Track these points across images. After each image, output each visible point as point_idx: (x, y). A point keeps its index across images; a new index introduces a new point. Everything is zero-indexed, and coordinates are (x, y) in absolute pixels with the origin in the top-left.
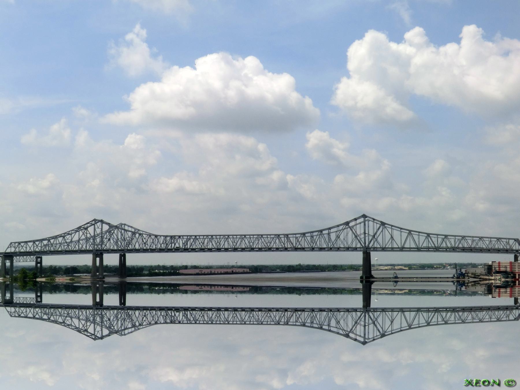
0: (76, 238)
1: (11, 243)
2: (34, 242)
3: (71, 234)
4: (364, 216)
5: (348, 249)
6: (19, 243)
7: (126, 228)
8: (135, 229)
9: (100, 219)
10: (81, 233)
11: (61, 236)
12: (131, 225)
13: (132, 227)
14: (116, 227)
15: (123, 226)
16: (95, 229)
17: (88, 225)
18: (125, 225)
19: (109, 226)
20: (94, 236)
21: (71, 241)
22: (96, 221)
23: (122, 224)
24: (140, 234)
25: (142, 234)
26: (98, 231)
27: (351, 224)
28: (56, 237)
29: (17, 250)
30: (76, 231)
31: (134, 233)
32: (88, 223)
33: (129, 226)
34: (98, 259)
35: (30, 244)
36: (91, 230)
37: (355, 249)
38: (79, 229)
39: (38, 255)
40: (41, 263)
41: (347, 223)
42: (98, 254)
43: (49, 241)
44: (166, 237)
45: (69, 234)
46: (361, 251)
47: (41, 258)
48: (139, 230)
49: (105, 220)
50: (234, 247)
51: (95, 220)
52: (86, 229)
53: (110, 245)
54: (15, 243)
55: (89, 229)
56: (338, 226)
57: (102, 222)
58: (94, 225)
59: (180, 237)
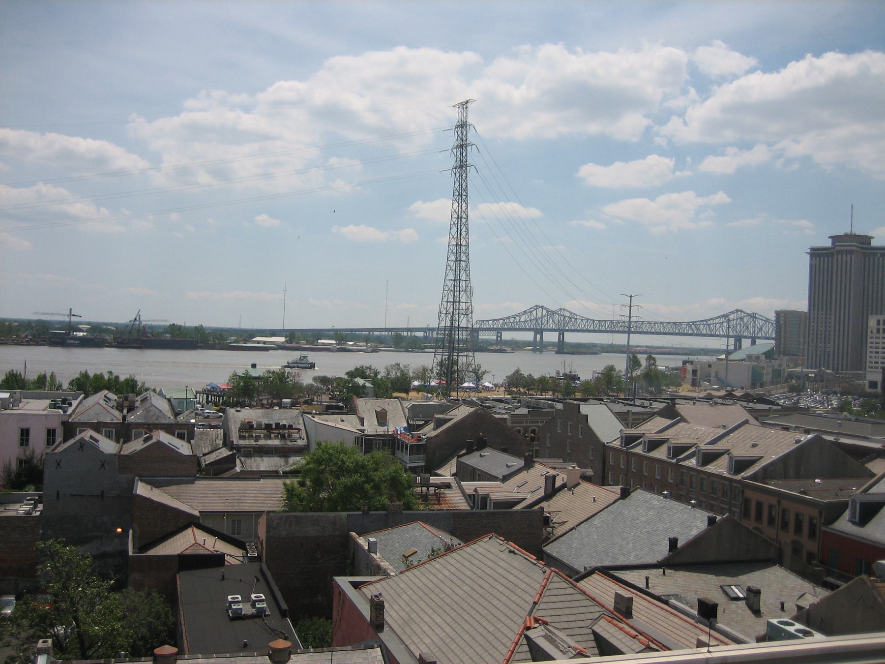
0: (523, 319)
1: (477, 321)
2: (493, 321)
4: (737, 311)
6: (483, 321)
9: (541, 305)
11: (512, 317)
13: (569, 312)
17: (532, 309)
18: (564, 309)
24: (576, 319)
26: (539, 315)
28: (508, 318)
29: (482, 326)
31: (570, 318)
32: (532, 308)
34: (538, 336)
35: (490, 322)
36: (534, 312)
38: (525, 312)
39: (499, 331)
40: (501, 337)
42: (539, 331)
43: (504, 320)
45: (518, 316)
47: (501, 333)
49: (545, 306)
51: (536, 306)
52: (531, 312)
53: (551, 325)
54: (480, 321)
56: (718, 317)
57: (542, 307)
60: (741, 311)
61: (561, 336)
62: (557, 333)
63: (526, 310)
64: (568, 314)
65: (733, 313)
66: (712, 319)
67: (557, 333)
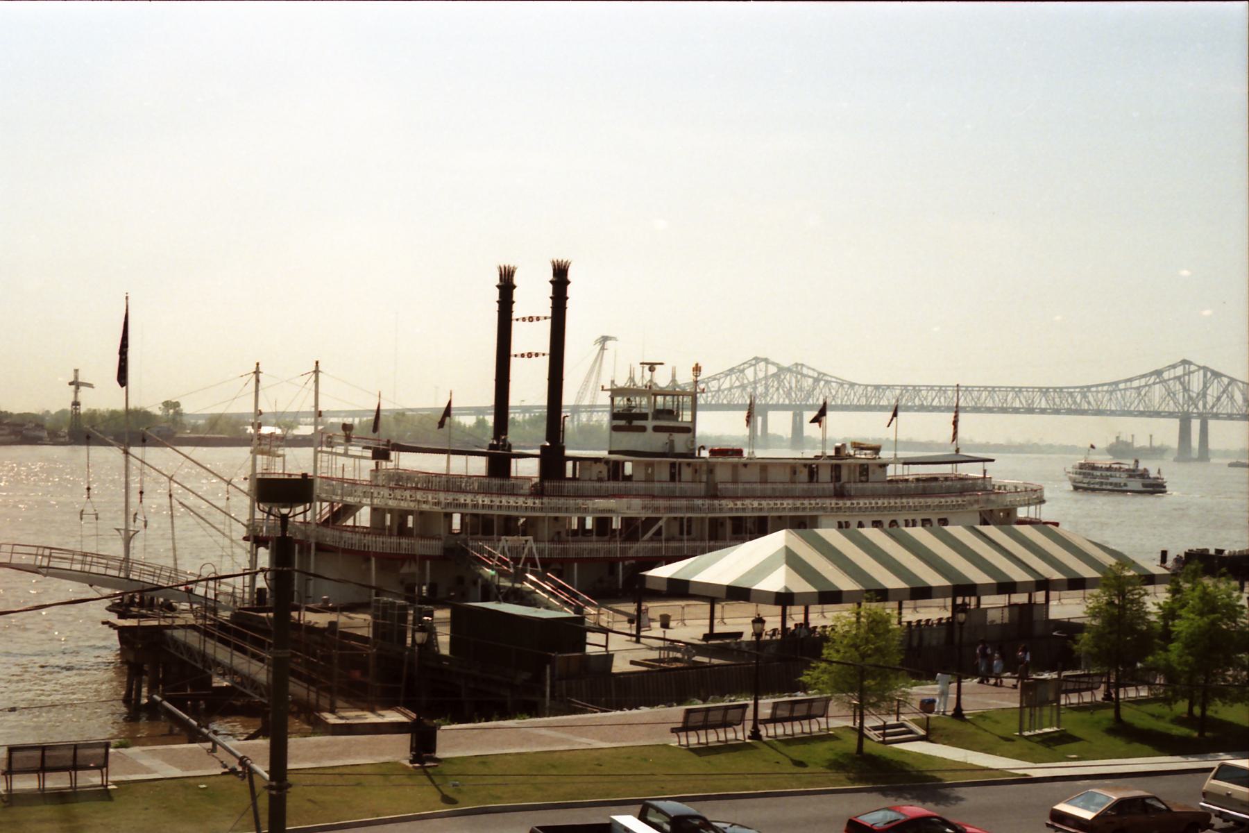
0: (726, 385)
3: (719, 380)
4: (1184, 362)
5: (1157, 414)
7: (805, 371)
8: (819, 373)
10: (734, 377)
12: (812, 367)
13: (813, 370)
14: (789, 370)
15: (799, 367)
16: (756, 373)
17: (746, 365)
19: (778, 368)
20: (755, 382)
21: (719, 389)
22: (757, 360)
23: (797, 364)
24: (827, 382)
25: (831, 382)
26: (761, 375)
27: (1166, 375)
30: (727, 375)
31: (817, 380)
33: (809, 368)
36: (750, 373)
37: (1171, 415)
41: (1158, 373)
44: (867, 386)
45: (714, 379)
46: (1177, 417)
48: (825, 375)
49: (772, 359)
50: (1000, 405)
51: (756, 359)
52: (742, 371)
55: (746, 371)
57: (766, 361)
58: (754, 365)
59: (888, 387)
60: (1190, 363)
61: (798, 418)
62: (789, 414)
63: (732, 371)
64: (811, 373)
65: (1174, 367)
66: (1130, 380)
67: (789, 414)
